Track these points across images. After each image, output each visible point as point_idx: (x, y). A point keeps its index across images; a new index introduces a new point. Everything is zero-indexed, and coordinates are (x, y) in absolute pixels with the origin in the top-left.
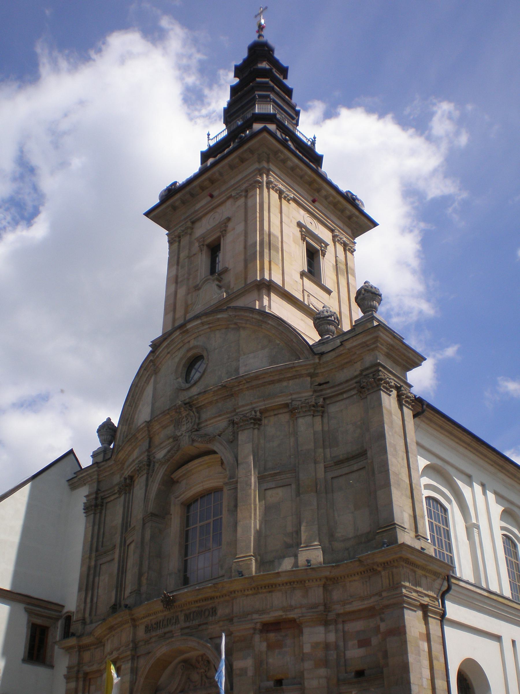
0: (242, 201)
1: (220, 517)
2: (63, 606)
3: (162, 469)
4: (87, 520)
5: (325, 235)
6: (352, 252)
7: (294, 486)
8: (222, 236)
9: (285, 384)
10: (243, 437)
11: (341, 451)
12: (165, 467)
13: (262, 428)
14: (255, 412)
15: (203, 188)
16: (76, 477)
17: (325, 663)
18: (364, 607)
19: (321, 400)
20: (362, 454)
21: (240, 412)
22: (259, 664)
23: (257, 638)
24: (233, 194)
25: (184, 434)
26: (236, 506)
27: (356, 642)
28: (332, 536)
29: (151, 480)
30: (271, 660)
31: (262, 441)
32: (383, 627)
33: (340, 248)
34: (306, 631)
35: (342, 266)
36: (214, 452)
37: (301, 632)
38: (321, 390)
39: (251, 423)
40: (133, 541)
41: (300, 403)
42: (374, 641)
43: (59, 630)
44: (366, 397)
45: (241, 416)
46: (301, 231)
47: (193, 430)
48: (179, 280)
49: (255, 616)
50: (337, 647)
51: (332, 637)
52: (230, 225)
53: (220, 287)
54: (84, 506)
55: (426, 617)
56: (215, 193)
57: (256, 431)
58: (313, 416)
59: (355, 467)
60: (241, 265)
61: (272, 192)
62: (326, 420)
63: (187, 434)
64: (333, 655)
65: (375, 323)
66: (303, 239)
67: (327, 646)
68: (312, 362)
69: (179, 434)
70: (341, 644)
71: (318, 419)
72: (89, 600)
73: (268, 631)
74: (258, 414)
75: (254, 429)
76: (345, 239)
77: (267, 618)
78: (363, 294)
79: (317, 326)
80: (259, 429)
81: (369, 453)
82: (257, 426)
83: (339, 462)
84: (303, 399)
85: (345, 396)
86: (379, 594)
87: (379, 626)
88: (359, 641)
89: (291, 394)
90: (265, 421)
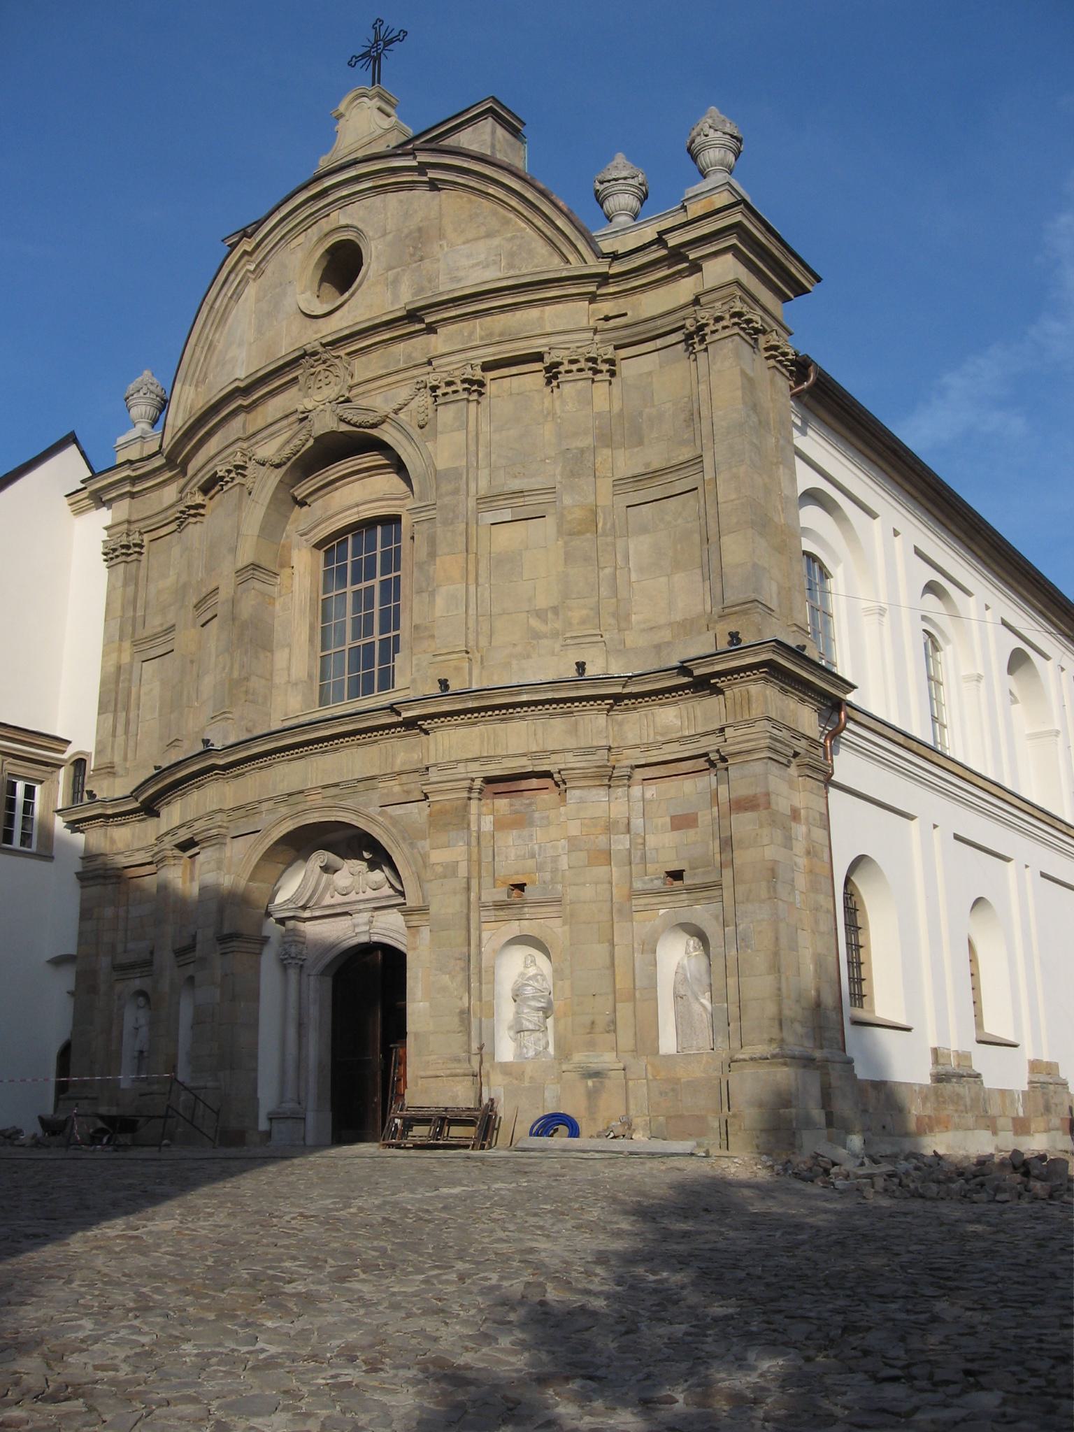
1: (393, 575)
3: (273, 476)
16: (85, 488)
17: (606, 856)
21: (440, 366)
25: (322, 407)
26: (432, 555)
27: (668, 819)
31: (485, 428)
39: (465, 389)
41: (567, 352)
45: (444, 375)
47: (342, 399)
49: (474, 766)
57: (473, 406)
58: (593, 381)
62: (616, 389)
64: (621, 843)
69: (310, 407)
71: (601, 389)
72: (120, 729)
75: (468, 401)
77: (495, 770)
78: (706, 136)
80: (478, 403)
82: (474, 396)
84: (573, 346)
88: (672, 818)
90: (491, 388)
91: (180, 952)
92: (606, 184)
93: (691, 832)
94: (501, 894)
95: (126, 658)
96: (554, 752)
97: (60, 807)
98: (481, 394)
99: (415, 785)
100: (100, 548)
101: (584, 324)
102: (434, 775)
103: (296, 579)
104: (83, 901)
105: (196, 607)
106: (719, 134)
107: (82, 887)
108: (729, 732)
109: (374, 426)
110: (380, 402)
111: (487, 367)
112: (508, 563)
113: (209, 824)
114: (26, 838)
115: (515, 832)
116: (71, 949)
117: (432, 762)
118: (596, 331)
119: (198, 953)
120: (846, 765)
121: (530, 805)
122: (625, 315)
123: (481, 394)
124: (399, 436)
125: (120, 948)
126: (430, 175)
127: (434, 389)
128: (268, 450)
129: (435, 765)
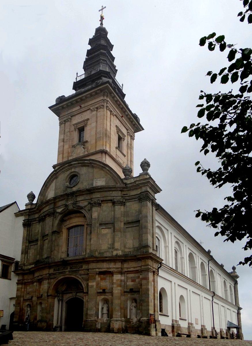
0: (95, 113)
2: (14, 259)
4: (24, 229)
5: (124, 131)
6: (133, 139)
7: (112, 229)
8: (85, 126)
9: (111, 192)
10: (94, 209)
11: (130, 219)
12: (61, 215)
13: (101, 207)
14: (99, 201)
15: (77, 102)
17: (120, 286)
18: (135, 270)
19: (124, 200)
20: (138, 221)
22: (98, 284)
23: (97, 276)
24: (91, 109)
26: (91, 233)
27: (131, 280)
28: (125, 247)
29: (54, 220)
30: (101, 283)
32: (141, 276)
33: (129, 138)
34: (115, 276)
35: (129, 145)
37: (113, 276)
38: (124, 197)
40: (47, 239)
42: (137, 280)
43: (13, 267)
44: (142, 202)
46: (117, 129)
48: (65, 141)
50: (124, 281)
51: (123, 278)
52: (89, 122)
53: (84, 148)
54: (23, 224)
55: (154, 275)
56: (83, 106)
59: (135, 225)
60: (94, 141)
61: (108, 111)
63: (71, 205)
64: (123, 283)
65: (148, 177)
66: (118, 133)
67: (121, 281)
68: (122, 186)
69: (68, 204)
70: (126, 280)
72: (26, 258)
74: (100, 202)
75: (98, 207)
76: (131, 134)
79: (124, 172)
81: (141, 222)
83: (129, 223)
84: (118, 199)
85: (133, 200)
86: (141, 267)
87: (139, 276)
89: (113, 197)
90: (102, 205)
91: (38, 298)
92: (124, 170)
93: (135, 282)
94: (101, 291)
95: (27, 244)
96: (112, 268)
97: (12, 270)
98: (101, 206)
99: (86, 272)
100: (22, 224)
102: (90, 270)
103: (63, 234)
104: (17, 288)
106: (146, 164)
107: (17, 285)
108: (142, 267)
109: (81, 209)
111: (102, 201)
112: (105, 235)
113: (46, 276)
115: (104, 281)
116: (15, 296)
117: (89, 268)
118: (122, 197)
119: (43, 298)
120: (161, 273)
121: (107, 276)
122: (127, 194)
124: (85, 212)
125: (25, 296)
126: (92, 165)
127: (92, 204)
128: (59, 210)
129: (90, 269)
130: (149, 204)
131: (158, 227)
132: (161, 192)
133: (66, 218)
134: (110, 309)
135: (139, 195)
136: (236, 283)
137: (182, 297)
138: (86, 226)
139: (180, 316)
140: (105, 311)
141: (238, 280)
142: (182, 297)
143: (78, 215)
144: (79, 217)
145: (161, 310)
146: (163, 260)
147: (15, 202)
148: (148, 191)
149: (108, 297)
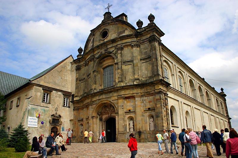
2: (72, 93)
36: (112, 56)
59: (148, 60)
73: (127, 99)
91: (86, 119)
97: (71, 101)
101: (136, 40)
105: (88, 76)
110: (111, 50)
114: (67, 105)
122: (141, 39)
123: (139, 46)
127: (117, 49)
128: (97, 56)
130: (156, 44)
131: (165, 61)
132: (164, 35)
133: (101, 61)
134: (135, 124)
135: (149, 39)
136: (225, 100)
137: (187, 112)
138: (114, 65)
139: (187, 127)
140: (132, 126)
141: (226, 97)
142: (187, 112)
143: (109, 58)
144: (110, 59)
145: (172, 124)
146: (171, 85)
147: (71, 55)
148: (155, 35)
149: (132, 115)
